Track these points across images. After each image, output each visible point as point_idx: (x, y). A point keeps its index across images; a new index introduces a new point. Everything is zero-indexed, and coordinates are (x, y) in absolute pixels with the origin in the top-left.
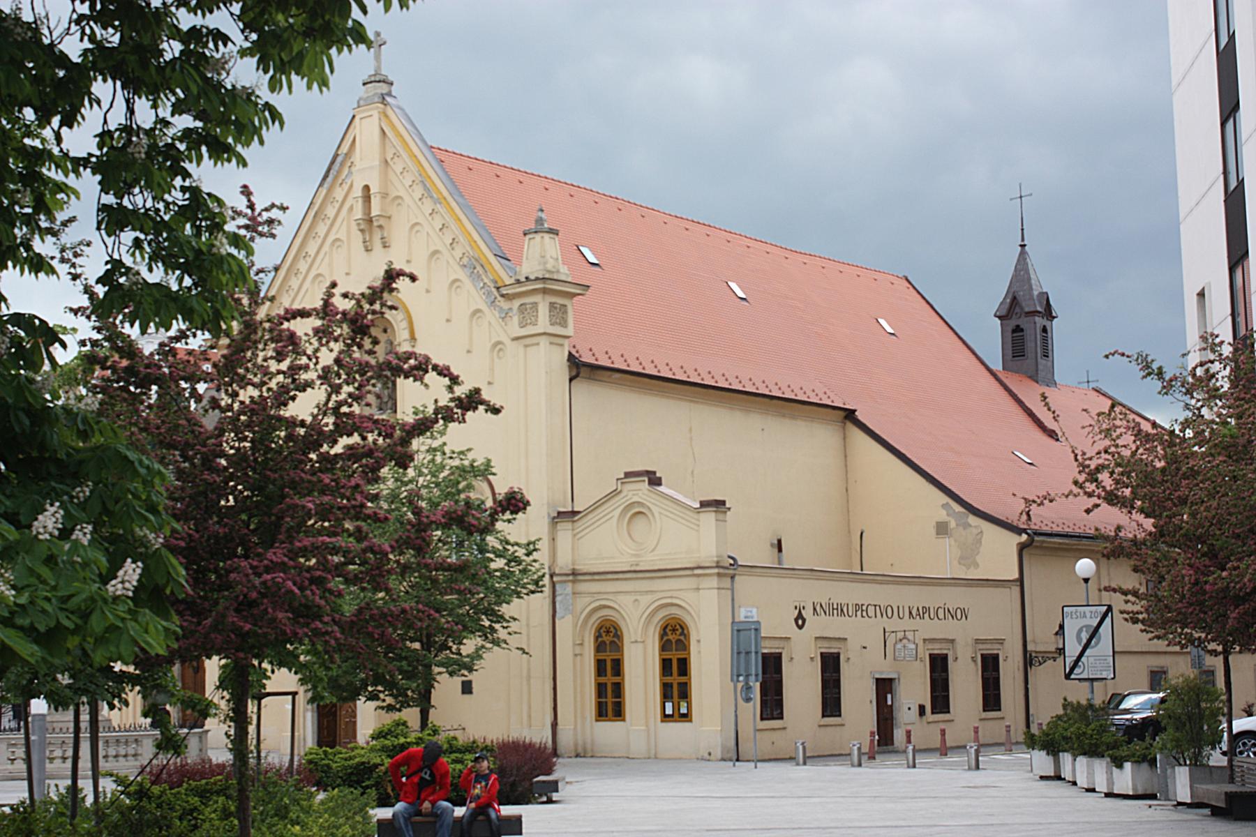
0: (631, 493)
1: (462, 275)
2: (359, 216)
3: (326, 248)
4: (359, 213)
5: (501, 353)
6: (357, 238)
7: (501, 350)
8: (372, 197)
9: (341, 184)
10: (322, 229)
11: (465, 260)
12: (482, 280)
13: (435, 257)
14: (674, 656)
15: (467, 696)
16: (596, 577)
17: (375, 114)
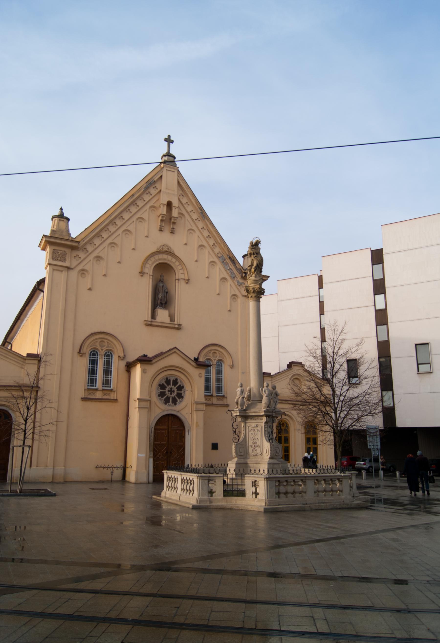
0: (296, 370)
1: (216, 260)
2: (165, 212)
3: (134, 218)
4: (164, 210)
5: (234, 300)
6: (155, 223)
7: (234, 298)
8: (173, 208)
9: (147, 193)
10: (133, 209)
11: (219, 255)
12: (229, 266)
13: (201, 247)
14: (312, 436)
15: (215, 451)
16: (283, 402)
17: (176, 172)
